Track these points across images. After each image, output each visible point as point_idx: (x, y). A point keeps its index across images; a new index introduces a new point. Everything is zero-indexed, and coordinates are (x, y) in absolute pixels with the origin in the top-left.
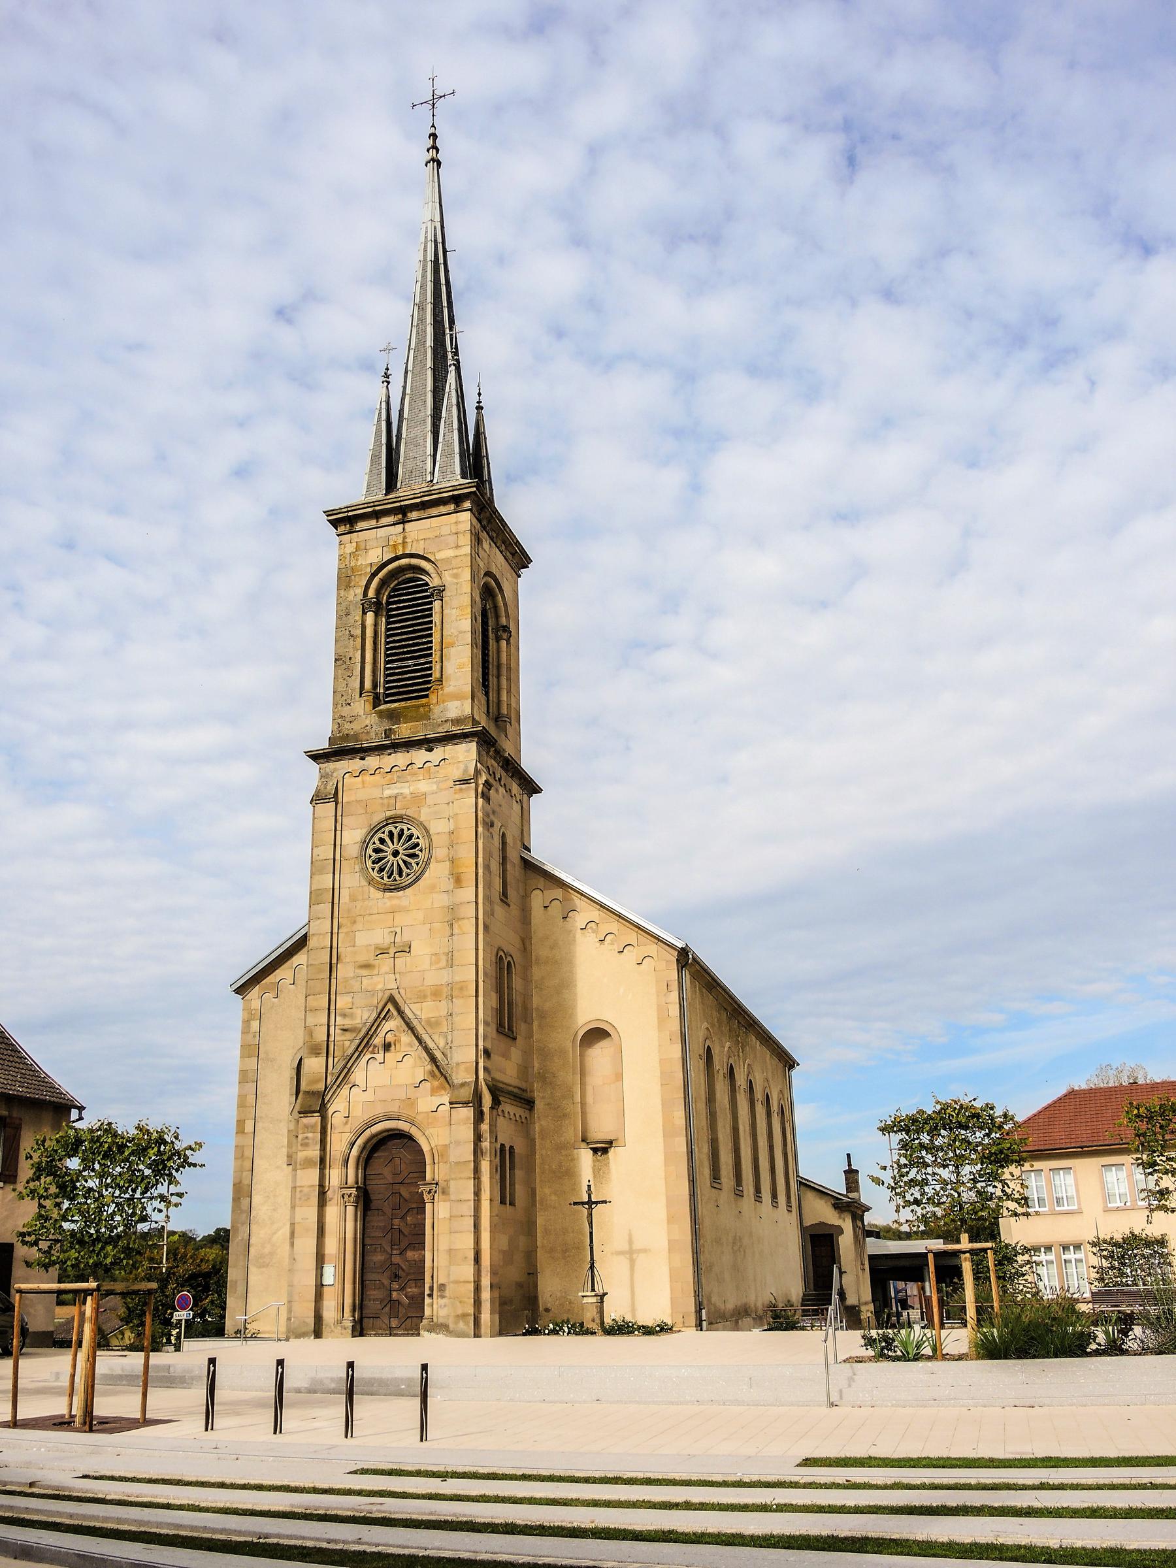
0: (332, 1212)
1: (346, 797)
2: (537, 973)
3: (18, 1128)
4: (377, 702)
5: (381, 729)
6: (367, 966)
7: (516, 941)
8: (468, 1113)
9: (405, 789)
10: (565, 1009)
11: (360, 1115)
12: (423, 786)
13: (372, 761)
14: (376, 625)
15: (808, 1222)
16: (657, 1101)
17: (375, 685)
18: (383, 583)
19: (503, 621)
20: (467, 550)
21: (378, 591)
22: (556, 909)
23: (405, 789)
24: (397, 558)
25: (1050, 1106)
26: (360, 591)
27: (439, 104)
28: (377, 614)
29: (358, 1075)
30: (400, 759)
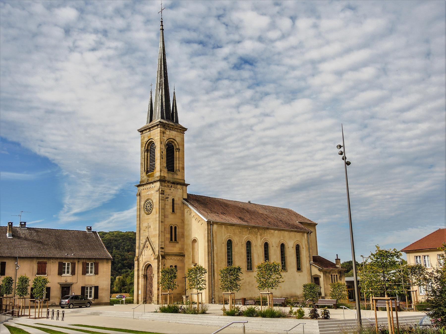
0: (140, 280)
1: (142, 195)
2: (186, 227)
3: (98, 264)
4: (147, 173)
5: (147, 179)
6: (145, 231)
7: (180, 221)
8: (156, 261)
9: (149, 193)
10: (190, 235)
11: (144, 261)
12: (152, 192)
13: (145, 187)
14: (147, 155)
15: (313, 274)
16: (203, 255)
17: (147, 169)
18: (148, 145)
19: (177, 147)
20: (159, 137)
21: (148, 147)
22: (188, 213)
23: (149, 193)
24: (149, 139)
25: (430, 235)
26: (144, 148)
27: (163, 11)
28: (147, 152)
29: (143, 253)
30: (148, 186)
